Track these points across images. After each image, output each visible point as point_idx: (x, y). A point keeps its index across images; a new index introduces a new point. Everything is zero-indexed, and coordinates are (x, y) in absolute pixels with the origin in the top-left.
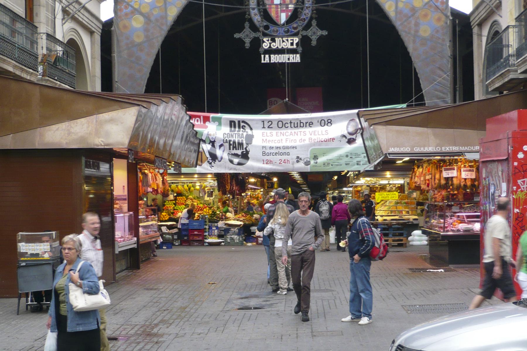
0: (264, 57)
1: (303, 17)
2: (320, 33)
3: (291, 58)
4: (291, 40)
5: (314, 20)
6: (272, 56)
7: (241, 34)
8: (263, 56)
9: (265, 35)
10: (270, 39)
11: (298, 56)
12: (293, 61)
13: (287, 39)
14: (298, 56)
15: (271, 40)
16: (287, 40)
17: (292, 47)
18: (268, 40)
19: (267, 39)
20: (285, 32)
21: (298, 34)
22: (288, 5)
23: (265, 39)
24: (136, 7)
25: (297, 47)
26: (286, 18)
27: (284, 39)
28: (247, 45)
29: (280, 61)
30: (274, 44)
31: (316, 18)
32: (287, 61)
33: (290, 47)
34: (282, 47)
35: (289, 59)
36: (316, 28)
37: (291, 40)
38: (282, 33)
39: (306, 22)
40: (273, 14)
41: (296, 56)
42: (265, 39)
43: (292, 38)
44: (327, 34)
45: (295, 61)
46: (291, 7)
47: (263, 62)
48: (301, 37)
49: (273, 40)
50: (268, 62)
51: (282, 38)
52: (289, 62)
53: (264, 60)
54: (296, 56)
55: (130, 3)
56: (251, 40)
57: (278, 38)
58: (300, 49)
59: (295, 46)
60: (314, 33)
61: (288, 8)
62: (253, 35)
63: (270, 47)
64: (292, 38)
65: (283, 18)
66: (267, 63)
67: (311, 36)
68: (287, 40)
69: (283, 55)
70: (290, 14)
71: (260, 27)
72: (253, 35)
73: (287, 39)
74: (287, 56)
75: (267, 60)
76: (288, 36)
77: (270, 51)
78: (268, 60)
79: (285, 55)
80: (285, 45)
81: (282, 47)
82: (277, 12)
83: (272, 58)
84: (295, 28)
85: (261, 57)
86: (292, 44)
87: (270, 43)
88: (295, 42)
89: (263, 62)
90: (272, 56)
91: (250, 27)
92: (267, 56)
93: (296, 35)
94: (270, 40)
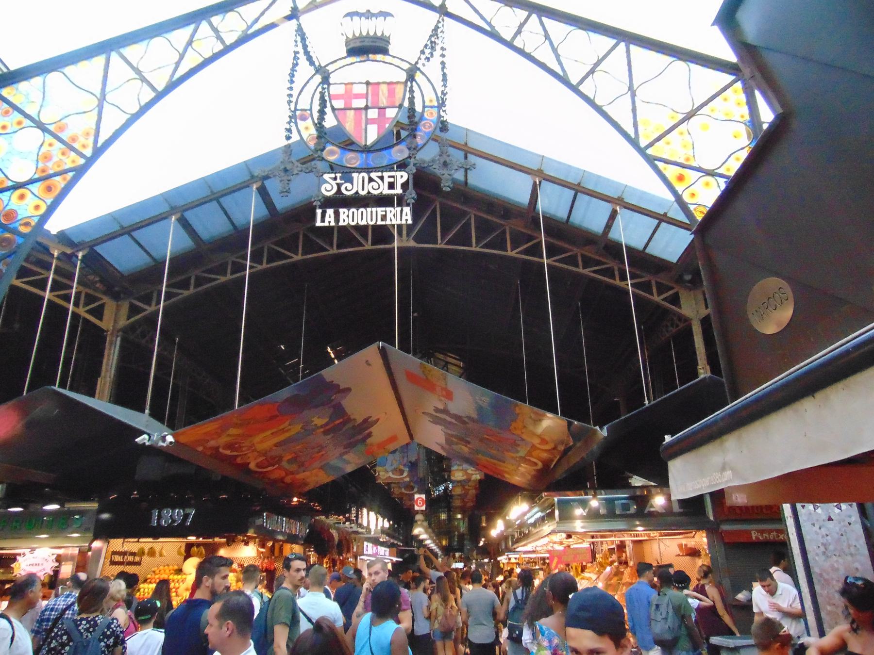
3: (389, 216)
4: (389, 177)
6: (341, 210)
8: (319, 212)
10: (338, 175)
13: (380, 174)
14: (407, 210)
15: (341, 179)
16: (382, 178)
18: (335, 179)
19: (333, 175)
22: (384, 108)
23: (326, 177)
24: (31, 111)
25: (403, 192)
26: (378, 134)
27: (374, 175)
29: (363, 223)
30: (349, 186)
32: (380, 223)
33: (386, 191)
34: (369, 192)
35: (384, 218)
37: (389, 177)
41: (402, 211)
46: (391, 113)
47: (319, 224)
48: (414, 171)
50: (333, 224)
51: (368, 173)
52: (383, 223)
53: (323, 220)
54: (402, 211)
55: (19, 106)
57: (360, 173)
58: (412, 194)
59: (398, 190)
65: (372, 135)
68: (382, 178)
69: (369, 210)
70: (387, 125)
73: (380, 174)
74: (380, 210)
75: (330, 219)
77: (339, 202)
78: (332, 219)
79: (374, 210)
80: (376, 186)
81: (369, 192)
82: (358, 122)
83: (342, 216)
86: (391, 186)
87: (339, 186)
88: (400, 182)
89: (319, 224)
90: (341, 210)
92: (330, 212)
93: (402, 166)
94: (338, 178)
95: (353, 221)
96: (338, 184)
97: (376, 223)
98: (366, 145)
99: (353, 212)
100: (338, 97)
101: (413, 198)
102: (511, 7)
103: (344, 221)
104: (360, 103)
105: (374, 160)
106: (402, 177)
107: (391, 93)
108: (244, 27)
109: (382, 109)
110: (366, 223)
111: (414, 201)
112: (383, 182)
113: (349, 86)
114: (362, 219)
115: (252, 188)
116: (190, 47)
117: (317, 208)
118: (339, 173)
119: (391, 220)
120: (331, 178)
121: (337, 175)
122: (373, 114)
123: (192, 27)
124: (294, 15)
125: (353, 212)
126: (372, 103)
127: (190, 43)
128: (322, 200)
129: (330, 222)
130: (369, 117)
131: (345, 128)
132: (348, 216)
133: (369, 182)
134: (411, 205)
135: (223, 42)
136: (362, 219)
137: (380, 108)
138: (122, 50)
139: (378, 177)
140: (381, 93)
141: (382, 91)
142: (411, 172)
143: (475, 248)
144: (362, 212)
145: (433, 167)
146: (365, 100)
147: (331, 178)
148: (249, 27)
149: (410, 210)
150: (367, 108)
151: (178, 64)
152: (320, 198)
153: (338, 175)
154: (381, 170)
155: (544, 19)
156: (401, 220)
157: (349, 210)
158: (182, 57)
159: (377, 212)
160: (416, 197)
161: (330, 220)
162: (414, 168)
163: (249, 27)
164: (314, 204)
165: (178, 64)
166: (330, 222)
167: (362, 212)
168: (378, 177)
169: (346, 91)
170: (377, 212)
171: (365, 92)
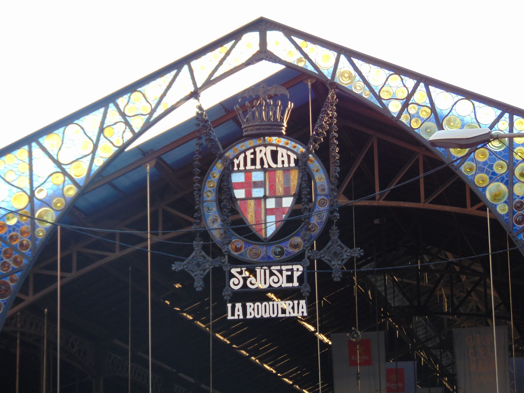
0: (233, 308)
1: (314, 220)
2: (347, 253)
4: (287, 270)
5: (334, 227)
6: (248, 304)
7: (184, 263)
8: (229, 305)
9: (236, 262)
11: (303, 302)
12: (292, 315)
14: (303, 302)
16: (281, 272)
17: (290, 285)
18: (240, 273)
19: (239, 270)
20: (275, 254)
21: (304, 258)
22: (281, 197)
23: (234, 271)
25: (300, 285)
28: (199, 285)
29: (267, 316)
31: (339, 225)
32: (280, 315)
33: (285, 285)
36: (340, 242)
37: (287, 270)
38: (269, 257)
39: (317, 232)
40: (250, 217)
42: (234, 271)
43: (290, 267)
44: (362, 254)
45: (295, 314)
46: (288, 202)
47: (230, 317)
49: (253, 273)
50: (241, 317)
51: (269, 267)
52: (283, 315)
53: (233, 314)
56: (205, 273)
58: (306, 289)
59: (296, 284)
60: (335, 254)
61: (279, 203)
62: (209, 264)
63: (245, 285)
64: (290, 267)
66: (239, 320)
67: (330, 262)
68: (281, 272)
70: (284, 216)
71: (224, 245)
72: (209, 264)
73: (278, 268)
75: (239, 313)
76: (281, 263)
78: (241, 313)
80: (276, 280)
81: (270, 286)
83: (249, 310)
84: (295, 246)
85: (227, 307)
86: (290, 279)
87: (245, 279)
88: (296, 275)
89: (230, 317)
90: (248, 304)
91: (205, 248)
95: (258, 314)
96: (243, 278)
97: (277, 316)
98: (266, 238)
99: (258, 306)
100: (240, 186)
101: (307, 291)
102: (399, 75)
103: (251, 314)
104: (258, 193)
105: (271, 251)
106: (298, 269)
107: (287, 180)
108: (149, 111)
109: (279, 199)
110: (269, 316)
111: (308, 294)
112: (282, 274)
113: (248, 174)
114: (265, 312)
115: (146, 167)
116: (102, 136)
117: (228, 302)
118: (244, 267)
119: (290, 313)
120: (238, 272)
121: (242, 269)
122: (271, 203)
123: (102, 110)
124: (195, 94)
125: (258, 306)
126: (270, 193)
127: (102, 130)
128: (231, 295)
129: (239, 315)
130: (268, 207)
131: (247, 220)
132: (254, 309)
133: (270, 276)
134: (306, 297)
135: (132, 130)
136: (265, 312)
137: (276, 197)
138: (41, 140)
139: (278, 270)
140: (277, 181)
141: (279, 179)
142: (305, 265)
143: (423, 205)
144: (265, 305)
145: (325, 258)
146: (262, 190)
147: (238, 272)
148: (153, 111)
149: (306, 303)
150: (265, 197)
151: (94, 152)
152: (229, 293)
153: (244, 269)
154: (280, 264)
155: (431, 88)
156: (298, 313)
157: (254, 304)
158: (96, 147)
159: (277, 305)
160: (310, 290)
161: (239, 313)
162: (308, 261)
163: (153, 111)
164: (225, 298)
165: (94, 152)
166: (239, 315)
167: (265, 305)
168: (278, 270)
169: (246, 179)
170: (277, 305)
171: (262, 179)
